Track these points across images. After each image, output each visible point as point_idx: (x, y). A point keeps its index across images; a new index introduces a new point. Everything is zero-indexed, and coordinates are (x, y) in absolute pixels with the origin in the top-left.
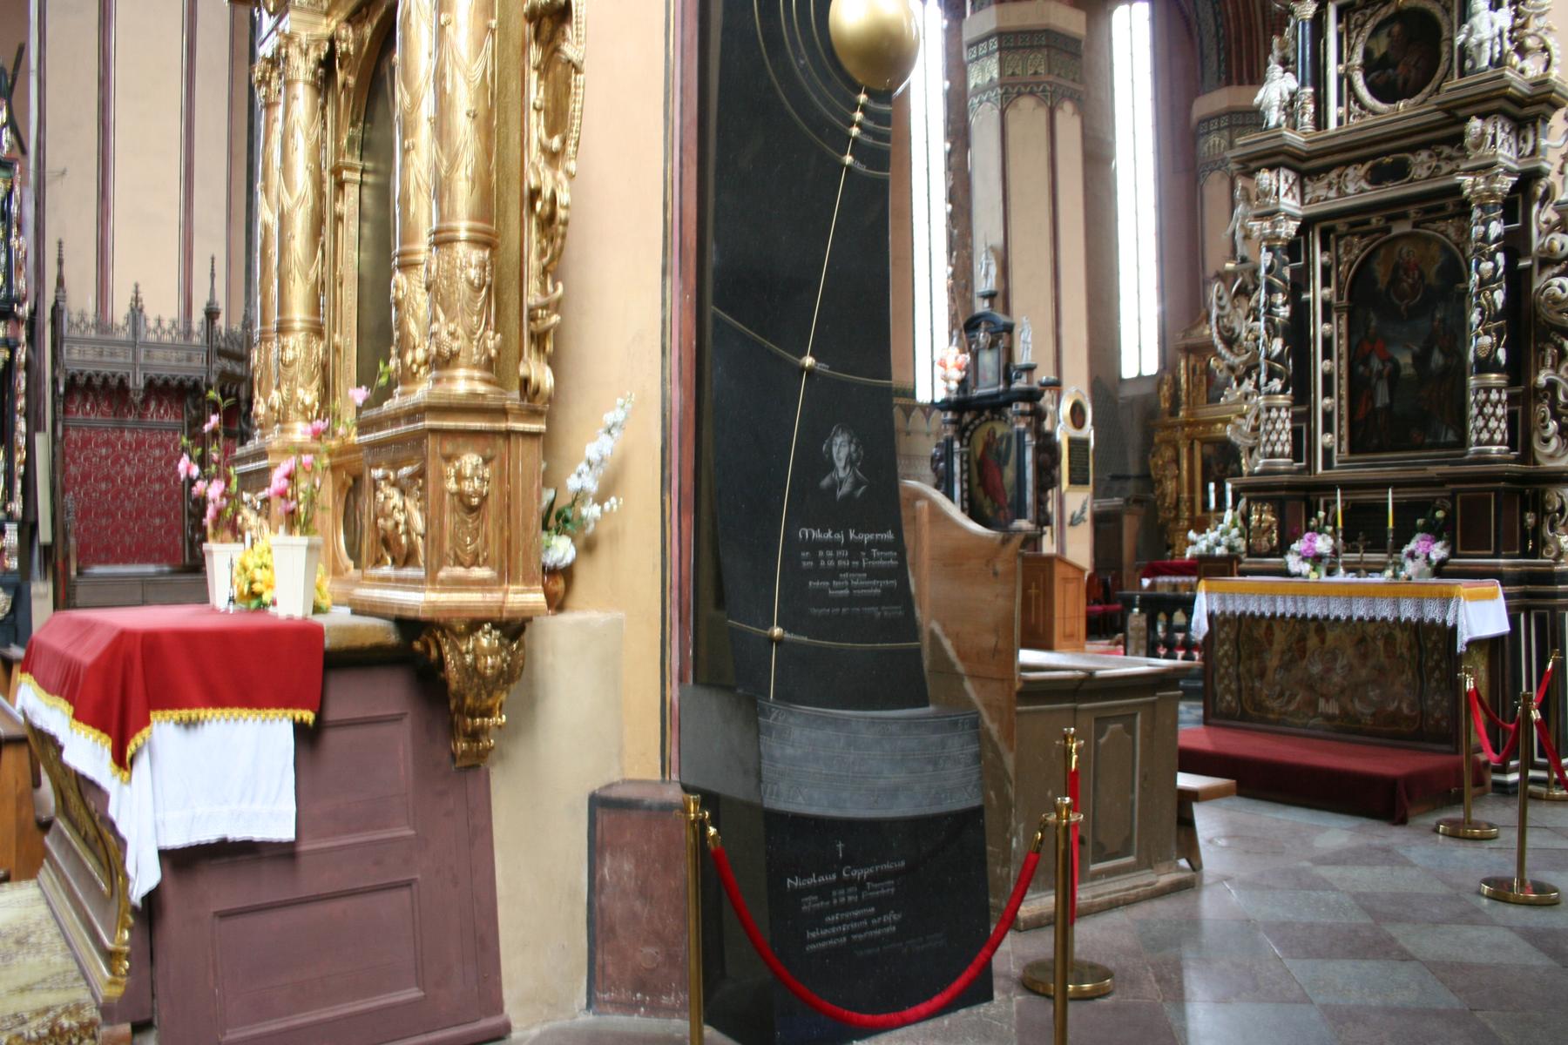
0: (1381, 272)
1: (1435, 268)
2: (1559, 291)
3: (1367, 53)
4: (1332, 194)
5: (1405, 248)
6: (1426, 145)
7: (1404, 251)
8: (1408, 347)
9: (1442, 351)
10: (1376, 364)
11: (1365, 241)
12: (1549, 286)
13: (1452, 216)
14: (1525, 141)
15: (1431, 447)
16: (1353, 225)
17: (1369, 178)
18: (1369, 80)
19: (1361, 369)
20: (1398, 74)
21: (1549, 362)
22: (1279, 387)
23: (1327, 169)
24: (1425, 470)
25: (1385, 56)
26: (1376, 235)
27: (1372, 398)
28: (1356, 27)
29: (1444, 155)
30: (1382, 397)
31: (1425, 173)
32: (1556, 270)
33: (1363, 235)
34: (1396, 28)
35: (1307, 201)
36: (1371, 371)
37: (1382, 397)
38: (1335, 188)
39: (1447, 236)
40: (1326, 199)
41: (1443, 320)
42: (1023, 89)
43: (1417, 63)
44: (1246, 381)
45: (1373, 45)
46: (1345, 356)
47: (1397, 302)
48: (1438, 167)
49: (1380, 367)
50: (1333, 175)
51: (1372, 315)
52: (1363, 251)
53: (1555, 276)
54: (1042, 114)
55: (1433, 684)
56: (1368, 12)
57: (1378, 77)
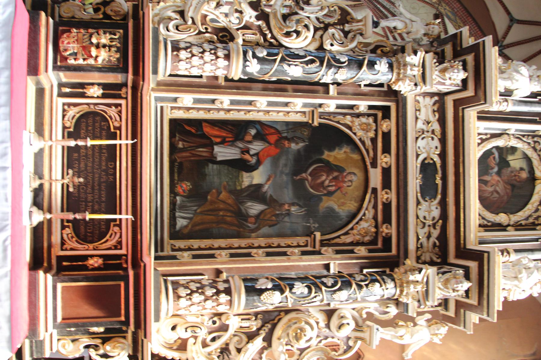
1: (336, 207)
3: (513, 150)
4: (420, 125)
6: (444, 216)
7: (354, 178)
8: (268, 180)
9: (262, 212)
10: (256, 147)
11: (368, 143)
15: (173, 203)
16: (386, 136)
17: (426, 162)
18: (494, 150)
19: (253, 132)
21: (246, 324)
22: (248, 69)
23: (442, 121)
25: (507, 164)
26: (371, 153)
27: (223, 142)
28: (535, 142)
29: (432, 230)
31: (421, 214)
32: (322, 324)
33: (374, 141)
35: (418, 98)
36: (250, 142)
38: (424, 127)
40: (417, 118)
41: (289, 214)
43: (497, 192)
44: (255, 14)
45: (518, 155)
47: (310, 170)
49: (252, 152)
50: (436, 127)
51: (301, 145)
57: (494, 158)
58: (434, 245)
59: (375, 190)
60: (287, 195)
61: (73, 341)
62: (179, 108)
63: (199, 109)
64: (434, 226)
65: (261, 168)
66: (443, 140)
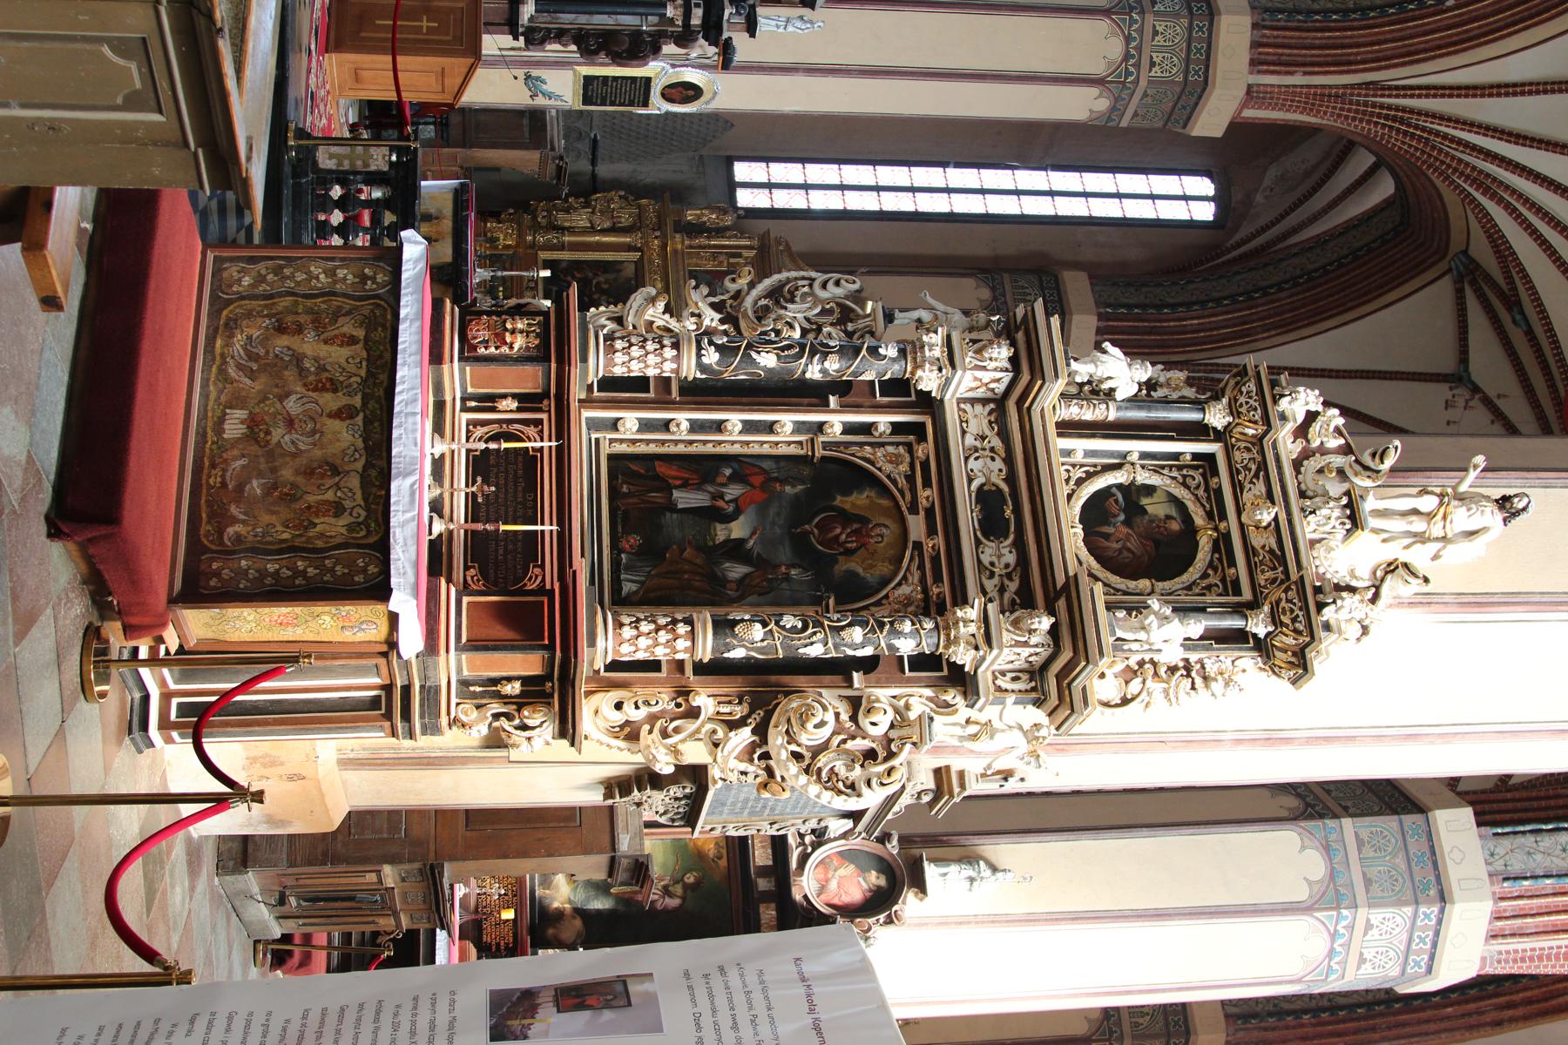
0: (858, 500)
1: (860, 571)
2: (816, 720)
3: (1149, 490)
5: (889, 532)
6: (1023, 560)
8: (753, 533)
9: (746, 576)
10: (733, 491)
11: (902, 482)
12: (825, 708)
13: (925, 591)
15: (616, 564)
16: (925, 465)
17: (986, 488)
18: (1114, 490)
19: (728, 472)
20: (1117, 528)
21: (725, 709)
22: (705, 360)
23: (1004, 435)
24: (583, 556)
26: (908, 496)
27: (685, 485)
28: (1184, 477)
29: (1006, 582)
30: (685, 499)
31: (986, 559)
32: (844, 717)
33: (910, 478)
34: (1175, 526)
35: (962, 406)
37: (685, 499)
38: (978, 444)
39: (900, 584)
40: (964, 432)
41: (787, 578)
42: (1133, 44)
43: (1129, 550)
44: (718, 316)
46: (745, 450)
47: (817, 520)
48: (992, 575)
50: (997, 442)
52: (888, 477)
53: (837, 715)
54: (1098, 68)
55: (271, 567)
56: (1201, 492)
57: (1116, 501)
59: (918, 546)
60: (784, 554)
61: (478, 707)
62: (622, 441)
63: (648, 442)
64: (1009, 576)
65: (742, 518)
66: (1009, 460)
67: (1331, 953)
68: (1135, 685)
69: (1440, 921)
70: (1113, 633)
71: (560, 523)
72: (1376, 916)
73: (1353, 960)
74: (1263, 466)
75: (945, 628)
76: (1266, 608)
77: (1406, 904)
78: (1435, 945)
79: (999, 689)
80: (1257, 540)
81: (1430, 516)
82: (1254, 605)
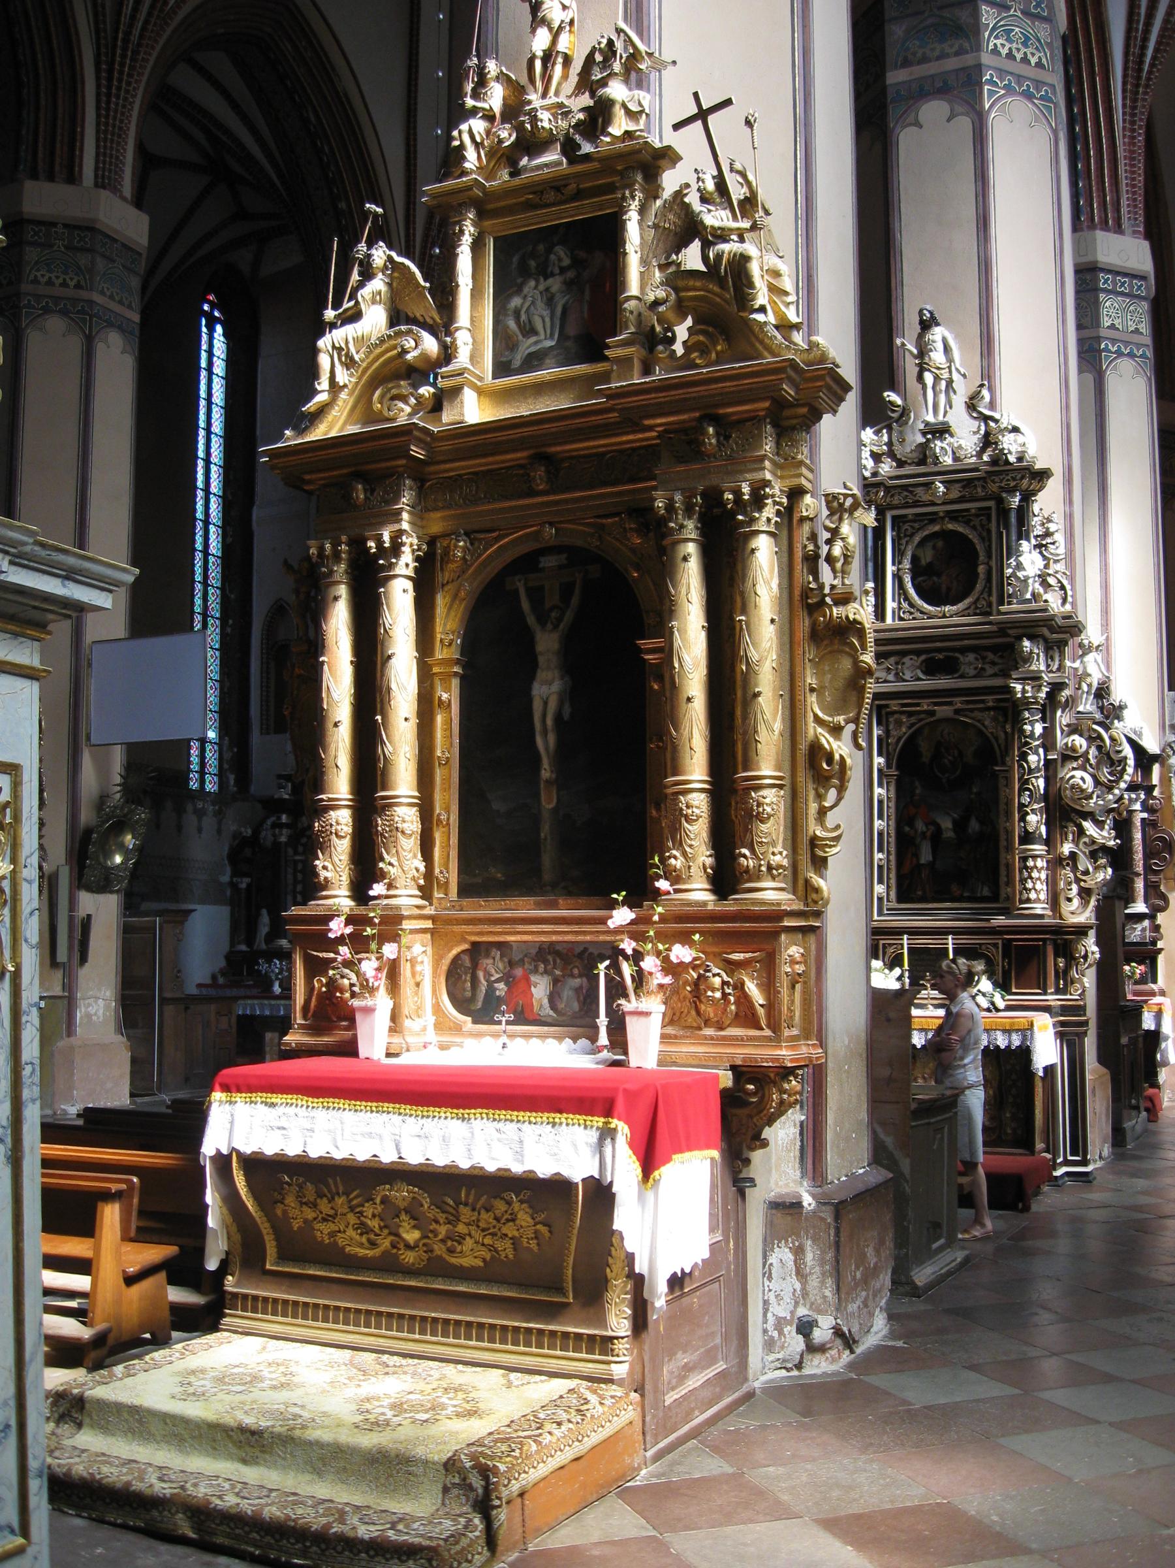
0: (925, 748)
2: (1081, 783)
3: (915, 560)
4: (891, 677)
7: (946, 731)
8: (948, 814)
10: (920, 826)
11: (913, 720)
12: (1073, 777)
13: (989, 709)
14: (1052, 659)
19: (907, 829)
21: (1070, 837)
24: (988, 920)
25: (930, 564)
26: (923, 716)
27: (916, 855)
28: (906, 536)
30: (926, 856)
31: (972, 672)
32: (1075, 765)
34: (940, 544)
36: (916, 831)
37: (926, 856)
39: (983, 724)
40: (886, 681)
45: (920, 553)
46: (893, 817)
48: (982, 669)
49: (924, 829)
50: (892, 660)
51: (917, 783)
52: (910, 728)
53: (1074, 769)
55: (1011, 1100)
56: (916, 525)
58: (1002, 657)
59: (957, 712)
61: (1072, 983)
62: (888, 894)
63: (888, 878)
64: (984, 658)
65: (939, 820)
66: (903, 654)
67: (1131, 355)
68: (1051, 580)
69: (1109, 271)
70: (1029, 601)
71: (947, 934)
72: (1106, 322)
73: (1136, 338)
74: (905, 487)
75: (1026, 703)
76: (1004, 495)
77: (1097, 298)
78: (1125, 275)
79: (1059, 670)
80: (955, 494)
81: (937, 378)
82: (1000, 501)
